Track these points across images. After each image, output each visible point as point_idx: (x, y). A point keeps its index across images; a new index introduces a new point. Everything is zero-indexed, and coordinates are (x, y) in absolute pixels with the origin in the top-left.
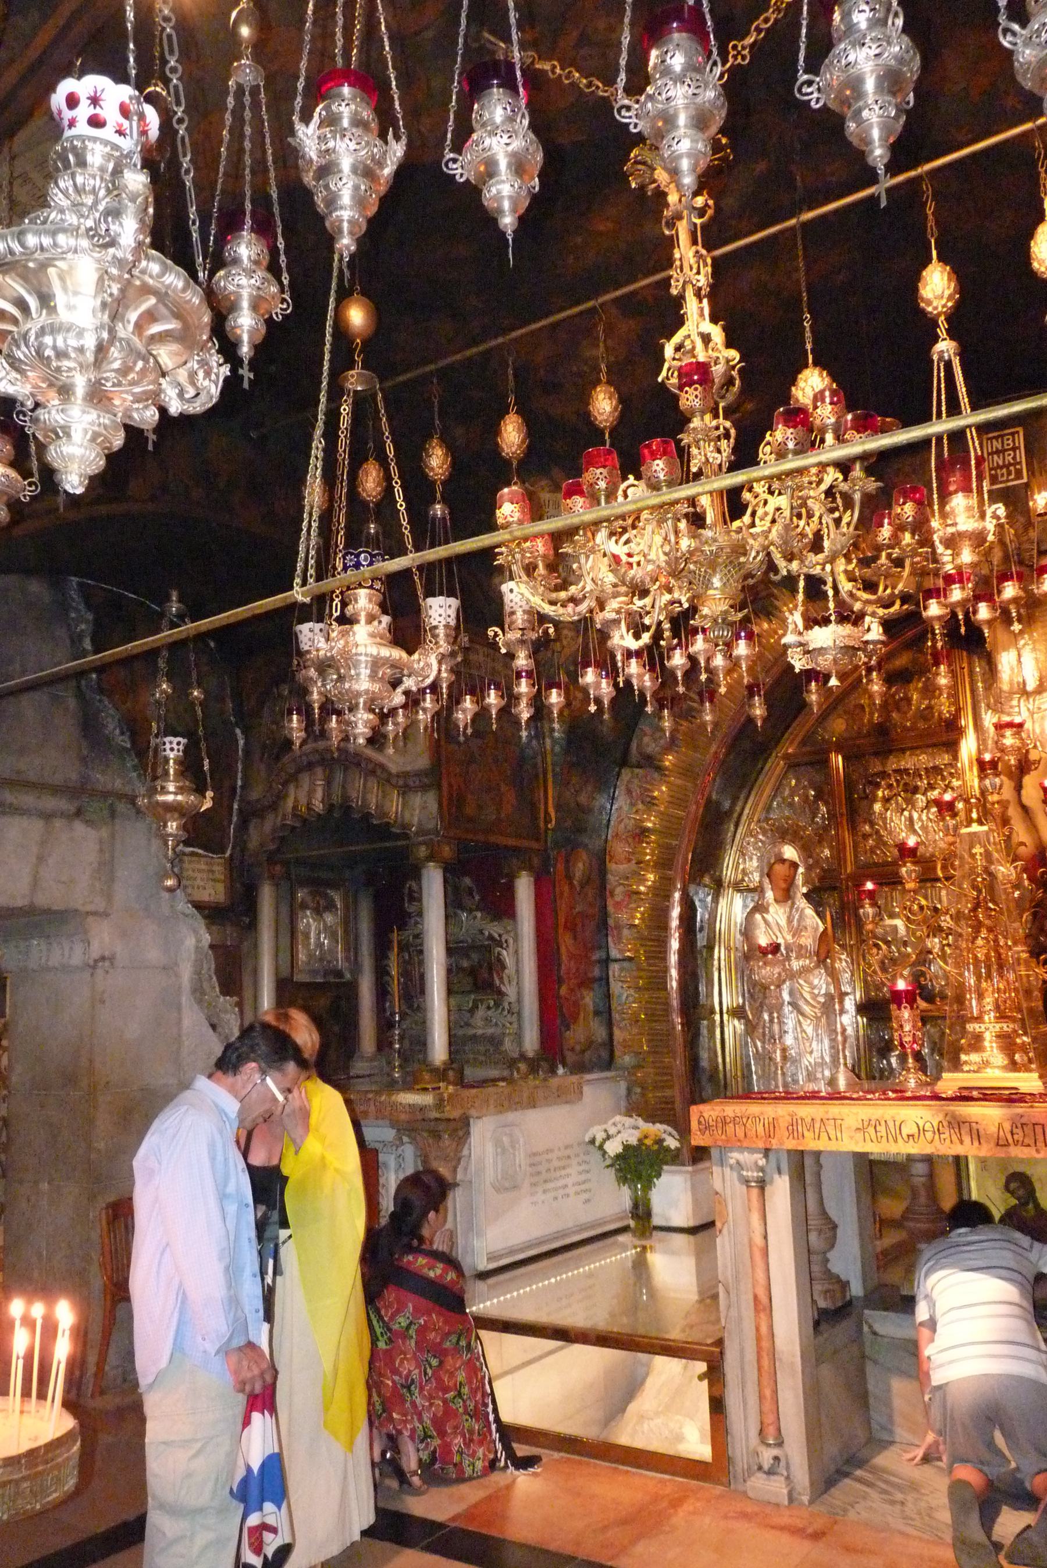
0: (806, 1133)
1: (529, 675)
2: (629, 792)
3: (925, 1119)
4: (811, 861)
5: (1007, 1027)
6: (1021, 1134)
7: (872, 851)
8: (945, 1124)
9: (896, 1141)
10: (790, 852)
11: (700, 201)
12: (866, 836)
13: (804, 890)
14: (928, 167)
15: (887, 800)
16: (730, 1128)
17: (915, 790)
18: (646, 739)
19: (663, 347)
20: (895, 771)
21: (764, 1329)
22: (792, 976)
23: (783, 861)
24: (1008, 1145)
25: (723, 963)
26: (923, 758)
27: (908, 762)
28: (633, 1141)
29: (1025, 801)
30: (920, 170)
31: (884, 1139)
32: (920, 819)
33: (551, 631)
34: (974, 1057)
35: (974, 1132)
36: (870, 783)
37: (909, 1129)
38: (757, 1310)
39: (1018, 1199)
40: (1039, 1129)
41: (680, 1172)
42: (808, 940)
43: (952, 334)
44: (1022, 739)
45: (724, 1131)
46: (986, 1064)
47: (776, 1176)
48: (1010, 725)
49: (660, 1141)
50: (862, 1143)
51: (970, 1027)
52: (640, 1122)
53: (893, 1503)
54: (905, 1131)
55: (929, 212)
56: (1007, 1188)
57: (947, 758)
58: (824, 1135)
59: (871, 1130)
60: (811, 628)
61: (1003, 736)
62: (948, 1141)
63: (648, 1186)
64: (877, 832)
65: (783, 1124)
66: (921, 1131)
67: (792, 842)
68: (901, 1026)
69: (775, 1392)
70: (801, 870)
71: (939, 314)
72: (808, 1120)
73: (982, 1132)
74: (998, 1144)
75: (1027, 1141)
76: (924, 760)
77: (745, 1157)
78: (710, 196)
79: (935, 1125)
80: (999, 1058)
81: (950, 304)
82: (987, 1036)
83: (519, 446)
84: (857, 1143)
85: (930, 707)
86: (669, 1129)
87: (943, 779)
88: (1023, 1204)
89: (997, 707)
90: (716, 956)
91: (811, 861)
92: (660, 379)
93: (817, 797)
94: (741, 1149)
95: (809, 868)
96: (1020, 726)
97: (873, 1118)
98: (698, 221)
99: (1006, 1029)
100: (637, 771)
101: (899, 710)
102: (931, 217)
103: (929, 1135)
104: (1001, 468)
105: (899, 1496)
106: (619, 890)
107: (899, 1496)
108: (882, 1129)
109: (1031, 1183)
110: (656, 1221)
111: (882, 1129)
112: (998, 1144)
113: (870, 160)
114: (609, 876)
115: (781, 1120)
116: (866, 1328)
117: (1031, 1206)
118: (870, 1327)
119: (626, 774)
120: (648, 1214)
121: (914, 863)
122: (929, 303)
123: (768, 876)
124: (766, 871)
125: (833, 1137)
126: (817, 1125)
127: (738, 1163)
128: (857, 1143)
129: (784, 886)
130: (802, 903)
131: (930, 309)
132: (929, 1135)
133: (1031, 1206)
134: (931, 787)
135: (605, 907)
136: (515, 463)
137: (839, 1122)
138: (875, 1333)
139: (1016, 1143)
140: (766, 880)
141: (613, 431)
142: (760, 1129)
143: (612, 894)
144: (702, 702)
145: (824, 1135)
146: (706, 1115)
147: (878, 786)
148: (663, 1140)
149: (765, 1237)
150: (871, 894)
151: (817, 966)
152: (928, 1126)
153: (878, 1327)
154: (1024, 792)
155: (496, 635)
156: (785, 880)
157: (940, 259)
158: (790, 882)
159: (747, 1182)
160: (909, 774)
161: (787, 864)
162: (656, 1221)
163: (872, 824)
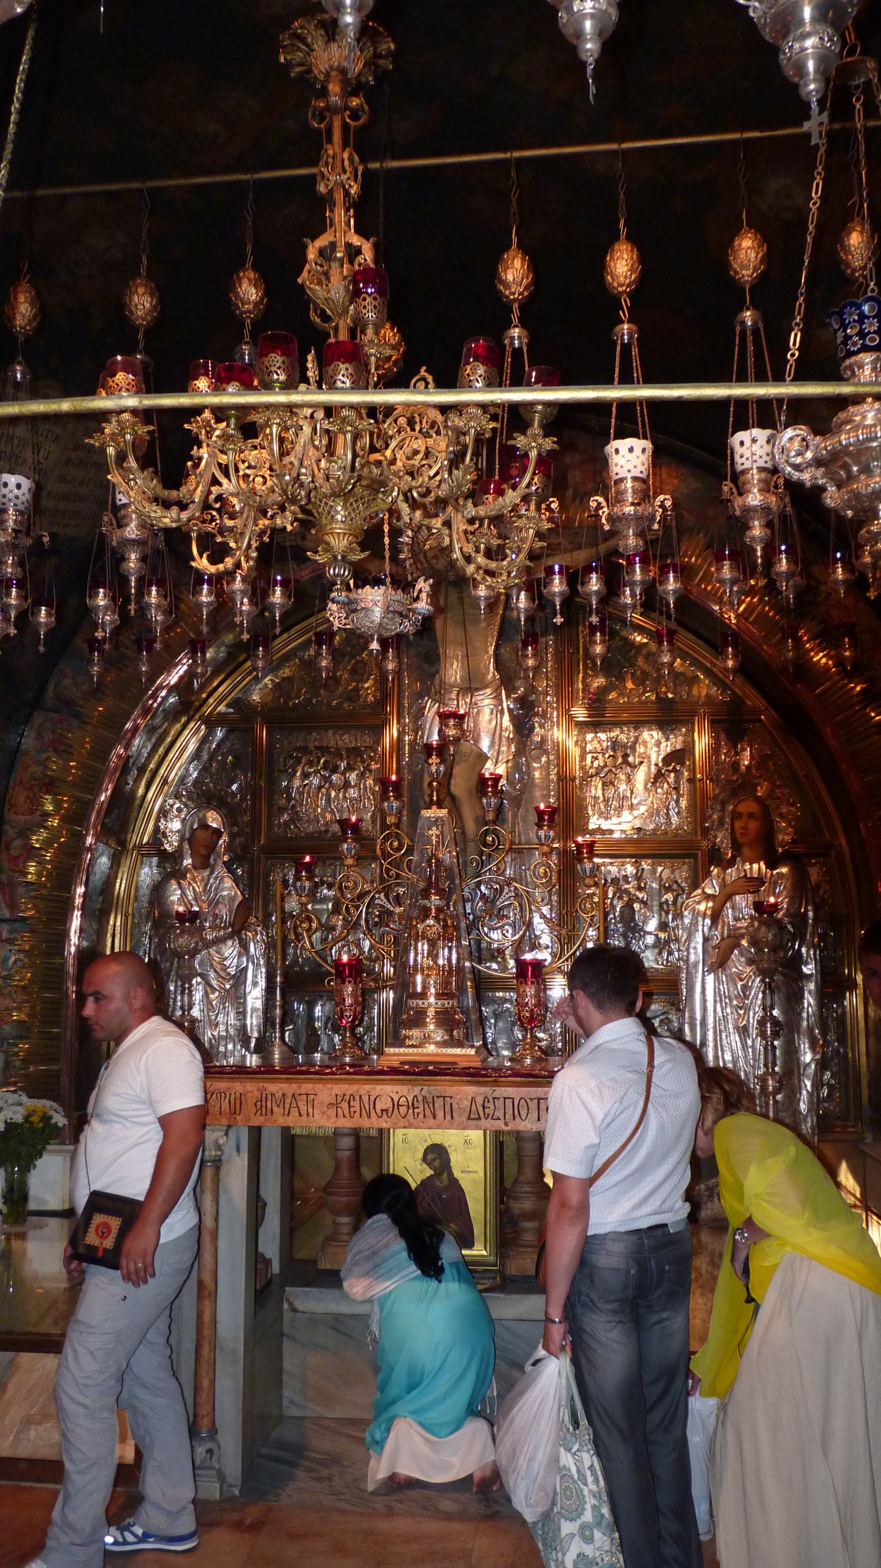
0: (275, 1109)
1: (20, 586)
2: (39, 737)
3: (400, 1094)
4: (235, 829)
5: (448, 1003)
6: (492, 1107)
7: (286, 824)
8: (420, 1098)
9: (369, 1117)
10: (214, 820)
11: (355, 102)
12: (282, 810)
13: (226, 858)
14: (517, 154)
15: (305, 776)
17: (335, 770)
18: (67, 682)
19: (305, 247)
20: (317, 748)
21: (207, 1317)
22: (208, 945)
23: (204, 826)
24: (479, 1118)
25: (118, 929)
26: (346, 737)
27: (332, 739)
28: (19, 1118)
29: (453, 789)
30: (508, 155)
31: (357, 1114)
32: (337, 796)
33: (46, 539)
34: (415, 1033)
35: (448, 1107)
36: (292, 757)
37: (387, 1104)
38: (200, 1296)
39: (434, 1169)
40: (509, 1103)
41: (61, 1151)
42: (224, 911)
43: (524, 323)
44: (462, 730)
46: (426, 1039)
48: (454, 715)
49: (46, 1118)
50: (334, 1119)
51: (413, 1003)
52: (24, 1098)
53: (320, 1480)
54: (379, 1106)
55: (514, 199)
56: (424, 1159)
57: (368, 740)
58: (294, 1111)
59: (345, 1105)
60: (363, 587)
61: (447, 726)
62: (421, 1116)
63: (27, 1166)
65: (252, 1098)
66: (396, 1105)
67: (217, 809)
68: (344, 1000)
69: (213, 1381)
70: (224, 838)
71: (515, 300)
73: (455, 1106)
74: (469, 1118)
75: (497, 1114)
76: (347, 740)
78: (368, 102)
79: (410, 1099)
80: (439, 1035)
81: (526, 293)
82: (431, 1012)
83: (30, 322)
84: (329, 1118)
85: (357, 690)
86: (55, 1105)
87: (363, 761)
88: (438, 1174)
89: (440, 697)
90: (111, 922)
91: (235, 829)
92: (300, 280)
93: (235, 765)
95: (232, 836)
96: (462, 717)
97: (348, 1093)
98: (353, 124)
99: (446, 1006)
100: (53, 715)
101: (326, 687)
102: (514, 204)
103: (403, 1110)
105: (325, 1472)
106: (17, 843)
107: (325, 1472)
108: (356, 1104)
109: (447, 1153)
110: (32, 1206)
111: (356, 1104)
112: (469, 1118)
113: (803, 92)
114: (7, 827)
115: (249, 1095)
116: (286, 1306)
117: (445, 1175)
118: (291, 1304)
119: (38, 718)
120: (25, 1197)
121: (355, 840)
122: (507, 286)
123: (189, 840)
124: (187, 836)
125: (304, 1112)
126: (288, 1101)
128: (329, 1118)
129: (204, 852)
130: (221, 870)
131: (507, 292)
132: (403, 1110)
133: (445, 1175)
134: (350, 768)
136: (21, 339)
138: (294, 1310)
140: (186, 846)
141: (149, 331)
142: (225, 1105)
143: (8, 848)
144: (140, 651)
145: (294, 1111)
147: (298, 761)
148: (51, 1118)
149: (216, 1219)
150: (309, 867)
151: (230, 936)
153: (298, 1304)
154: (453, 782)
157: (519, 246)
158: (212, 847)
160: (329, 753)
161: (210, 831)
162: (32, 1206)
163: (289, 798)
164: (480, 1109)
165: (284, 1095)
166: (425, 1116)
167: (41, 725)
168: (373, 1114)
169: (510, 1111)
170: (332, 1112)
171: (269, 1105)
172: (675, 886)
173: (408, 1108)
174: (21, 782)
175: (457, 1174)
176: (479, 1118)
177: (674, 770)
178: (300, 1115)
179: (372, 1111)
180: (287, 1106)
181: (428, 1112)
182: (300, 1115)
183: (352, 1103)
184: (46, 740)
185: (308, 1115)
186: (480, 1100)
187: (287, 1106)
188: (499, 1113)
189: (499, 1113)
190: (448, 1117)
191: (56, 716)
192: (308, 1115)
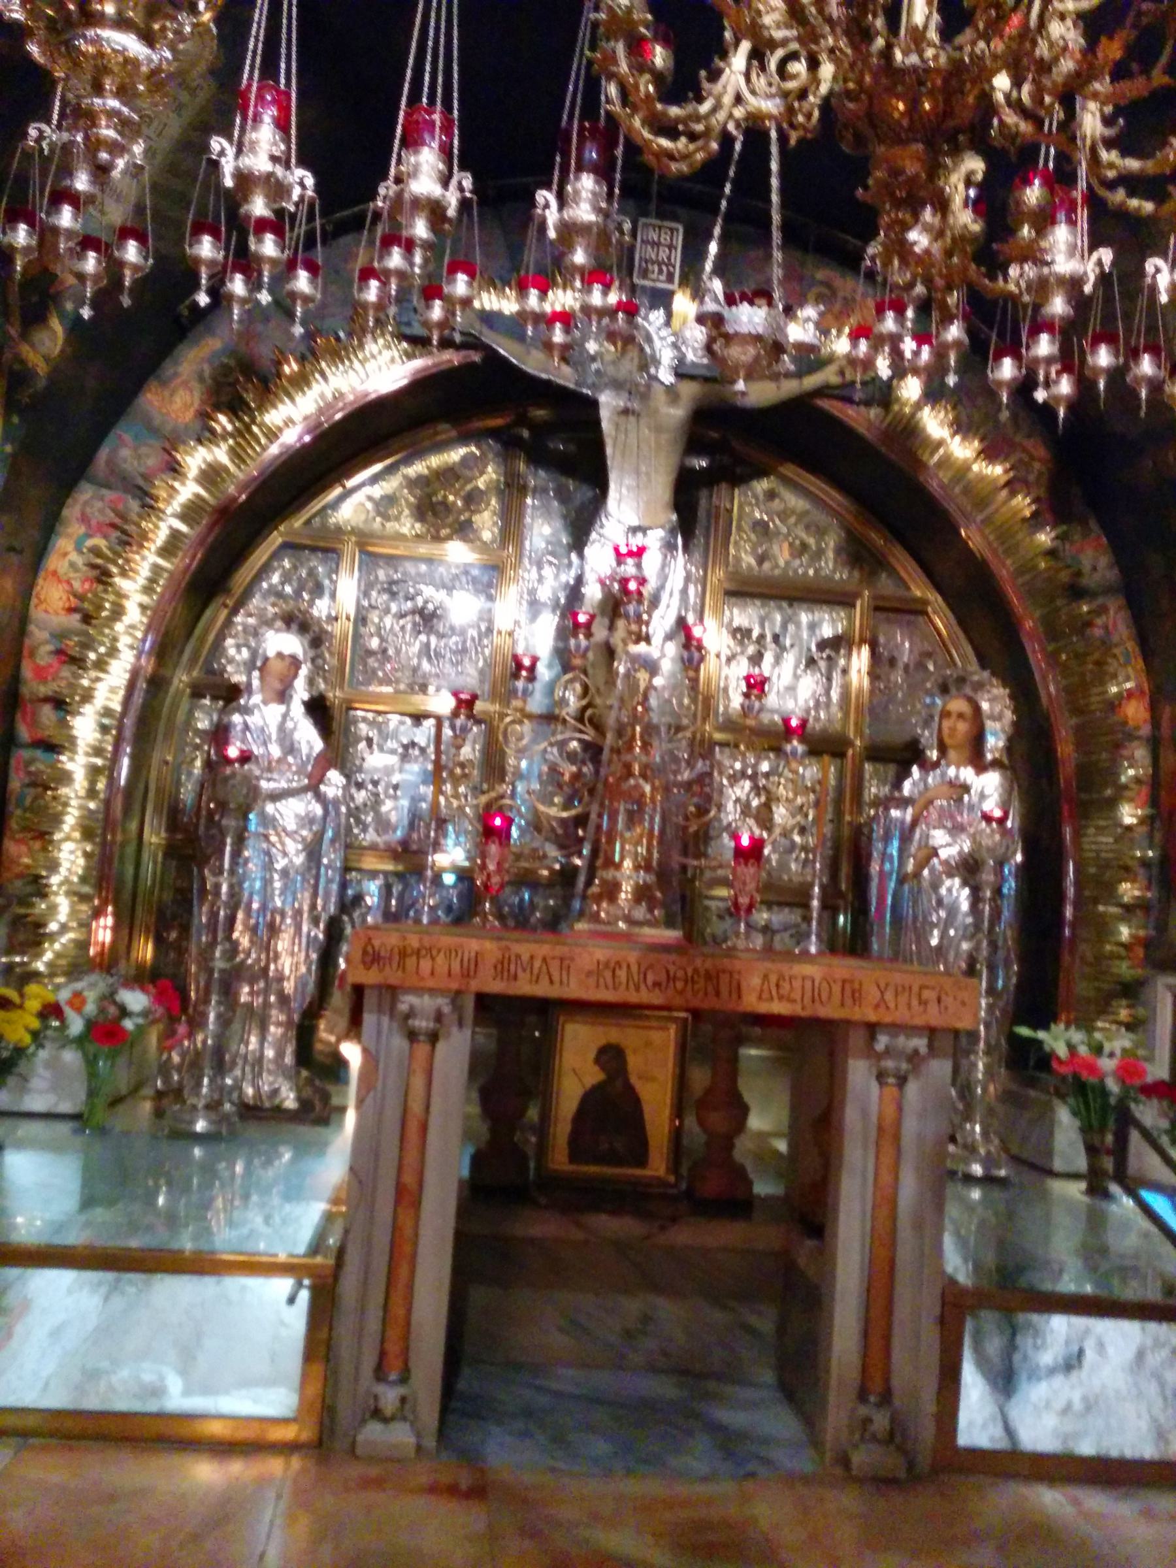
0: (520, 974)
8: (702, 972)
9: (637, 989)
16: (411, 962)
18: (125, 453)
31: (624, 986)
40: (808, 984)
45: (402, 966)
47: (455, 1030)
56: (597, 1061)
58: (545, 980)
59: (608, 974)
62: (701, 994)
64: (385, 651)
72: (525, 958)
77: (426, 1003)
79: (690, 972)
94: (418, 991)
100: (104, 492)
104: (653, 263)
108: (622, 974)
111: (622, 974)
114: (32, 628)
125: (556, 978)
126: (537, 964)
127: (412, 1007)
135: (18, 667)
137: (566, 963)
139: (781, 998)
142: (456, 966)
143: (32, 654)
146: (376, 943)
152: (680, 974)
155: (222, 153)
156: (281, 681)
159: (412, 1036)
164: (774, 992)
165: (532, 957)
166: (706, 994)
167: (86, 503)
168: (643, 987)
169: (808, 994)
170: (592, 981)
171: (512, 967)
172: (818, 787)
173: (686, 982)
174: (55, 573)
175: (633, 1080)
176: (772, 998)
177: (829, 658)
178: (551, 982)
179: (643, 987)
180: (536, 971)
181: (710, 989)
182: (551, 982)
183: (618, 972)
184: (94, 523)
185: (561, 982)
186: (773, 978)
187: (536, 971)
188: (797, 995)
189: (797, 995)
190: (734, 996)
191: (108, 494)
192: (561, 982)
